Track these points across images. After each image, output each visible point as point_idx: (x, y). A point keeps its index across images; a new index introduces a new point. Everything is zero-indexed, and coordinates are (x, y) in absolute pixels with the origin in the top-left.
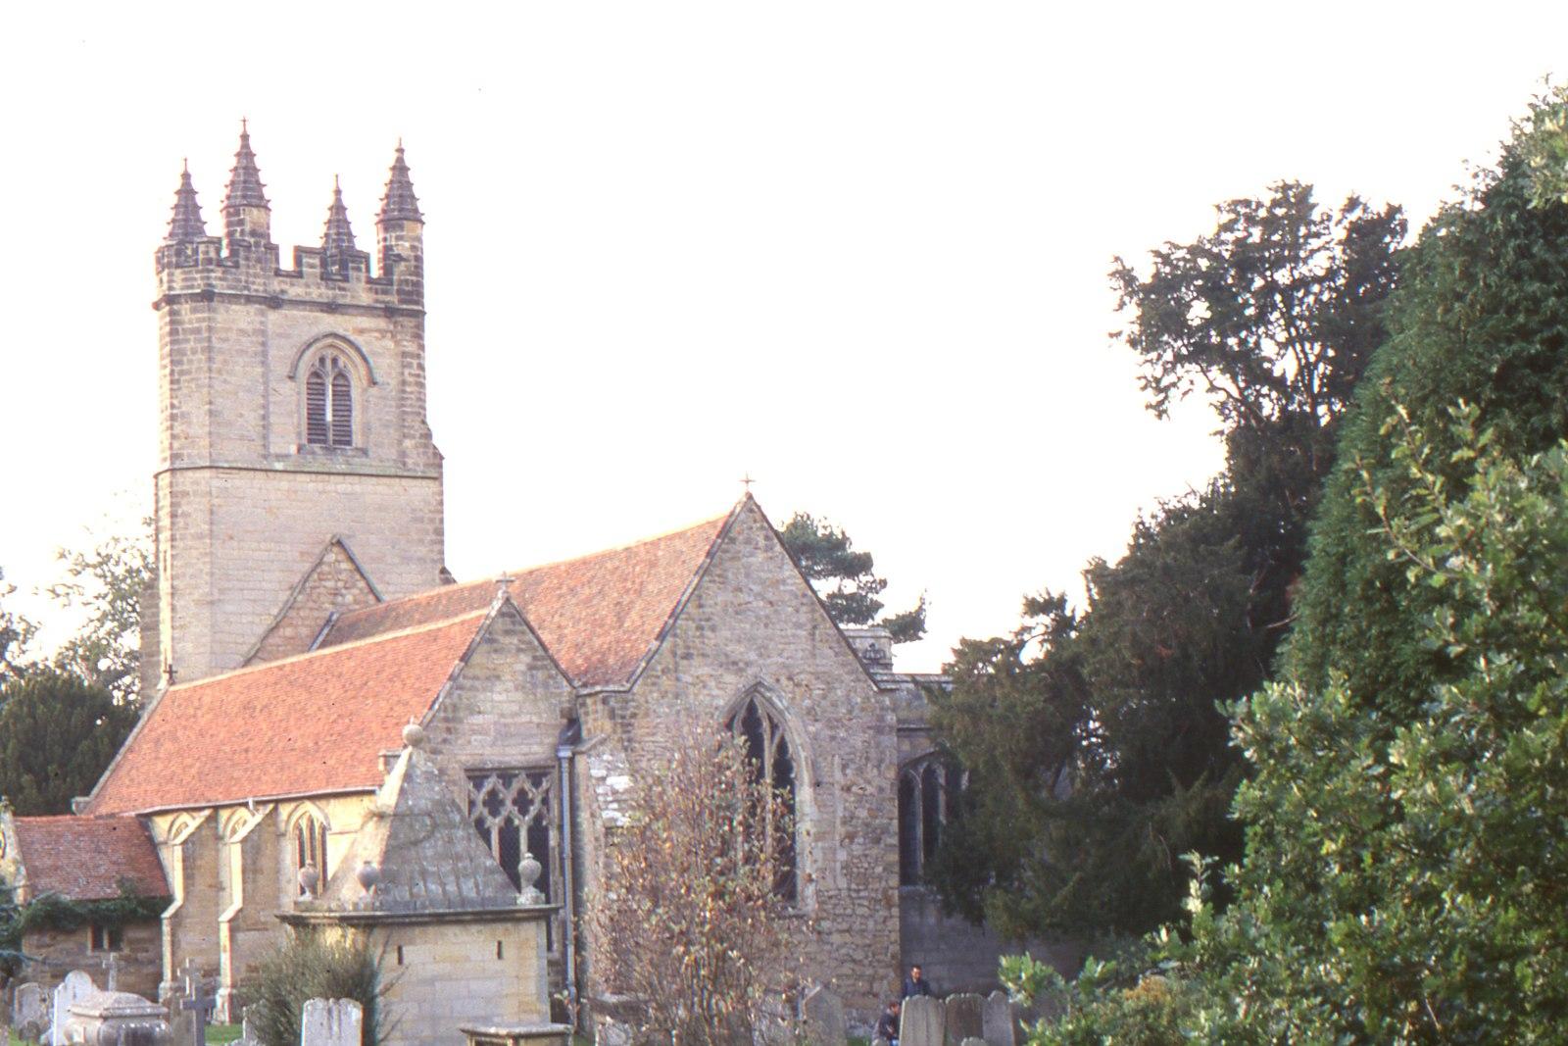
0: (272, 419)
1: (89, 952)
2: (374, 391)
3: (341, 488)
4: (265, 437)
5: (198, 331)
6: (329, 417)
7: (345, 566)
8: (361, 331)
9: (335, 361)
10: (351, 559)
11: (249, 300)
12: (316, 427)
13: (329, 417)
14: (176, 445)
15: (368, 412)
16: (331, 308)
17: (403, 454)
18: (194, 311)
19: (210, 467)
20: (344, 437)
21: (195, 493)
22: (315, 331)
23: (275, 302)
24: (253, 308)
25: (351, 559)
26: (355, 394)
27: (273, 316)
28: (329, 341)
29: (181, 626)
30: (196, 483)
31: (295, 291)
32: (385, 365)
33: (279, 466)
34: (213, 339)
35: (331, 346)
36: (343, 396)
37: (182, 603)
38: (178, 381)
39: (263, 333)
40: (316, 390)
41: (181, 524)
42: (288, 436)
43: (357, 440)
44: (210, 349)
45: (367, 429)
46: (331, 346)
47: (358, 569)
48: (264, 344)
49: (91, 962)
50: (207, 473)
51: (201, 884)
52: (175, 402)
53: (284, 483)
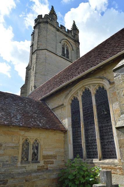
0: (57, 48)
1: (19, 164)
4: (56, 49)
5: (45, 28)
6: (65, 53)
8: (71, 42)
9: (66, 45)
11: (54, 27)
12: (63, 54)
13: (65, 53)
14: (38, 46)
16: (67, 36)
18: (44, 25)
19: (46, 49)
20: (68, 57)
21: (42, 54)
22: (65, 38)
23: (58, 30)
24: (55, 29)
26: (70, 51)
27: (57, 32)
28: (66, 41)
29: (37, 80)
30: (43, 52)
31: (60, 30)
34: (48, 30)
35: (66, 42)
36: (67, 51)
37: (38, 75)
38: (40, 36)
39: (56, 33)
40: (63, 48)
41: (38, 60)
42: (60, 54)
43: (70, 58)
44: (47, 30)
45: (71, 57)
46: (66, 42)
48: (56, 35)
49: (20, 171)
50: (46, 51)
52: (39, 39)
53: (60, 58)
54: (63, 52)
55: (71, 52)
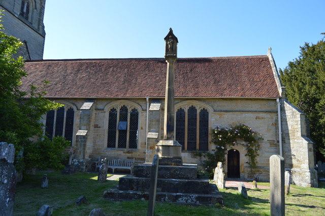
2: (35, 10)
3: (27, 29)
6: (25, 11)
7: (25, 49)
10: (27, 48)
12: (22, 14)
13: (25, 11)
15: (33, 15)
17: (39, 28)
20: (27, 18)
25: (27, 48)
26: (31, 9)
32: (38, 6)
33: (17, 16)
36: (28, 7)
43: (30, 20)
47: (28, 51)
51: (92, 124)
53: (17, 21)
54: (22, 8)
55: (33, 11)
